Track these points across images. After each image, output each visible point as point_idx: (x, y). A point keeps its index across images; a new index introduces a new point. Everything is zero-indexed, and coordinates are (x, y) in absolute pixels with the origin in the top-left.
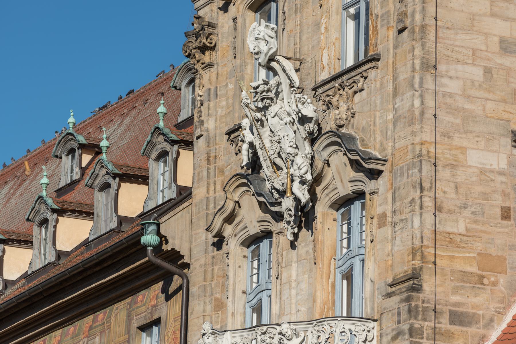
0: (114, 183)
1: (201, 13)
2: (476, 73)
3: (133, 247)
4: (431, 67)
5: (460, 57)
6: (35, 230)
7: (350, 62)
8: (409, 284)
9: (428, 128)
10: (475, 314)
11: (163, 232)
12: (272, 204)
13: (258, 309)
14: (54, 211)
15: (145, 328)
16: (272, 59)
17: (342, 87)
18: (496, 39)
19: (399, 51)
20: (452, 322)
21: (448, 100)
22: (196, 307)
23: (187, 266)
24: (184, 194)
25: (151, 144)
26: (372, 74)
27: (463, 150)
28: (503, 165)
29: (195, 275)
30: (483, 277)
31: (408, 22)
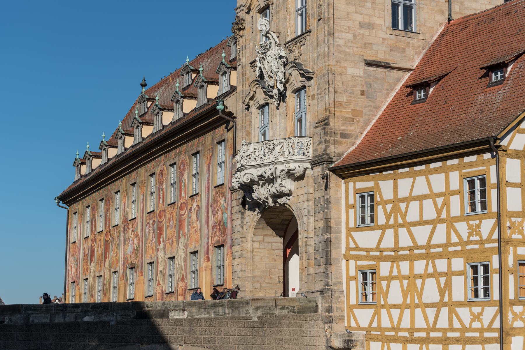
0: (205, 85)
1: (238, 15)
2: (350, 36)
3: (213, 111)
4: (332, 34)
5: (343, 30)
6: (175, 105)
7: (299, 33)
8: (324, 122)
9: (331, 59)
10: (351, 134)
11: (225, 104)
12: (269, 92)
13: (264, 134)
14: (182, 97)
15: (219, 143)
16: (267, 33)
17: (296, 43)
18: (358, 22)
19: (319, 28)
20: (342, 137)
21: (339, 48)
22: (239, 134)
23: (235, 118)
24: (233, 89)
25: (220, 69)
26: (308, 38)
28: (361, 73)
29: (239, 121)
31: (322, 16)
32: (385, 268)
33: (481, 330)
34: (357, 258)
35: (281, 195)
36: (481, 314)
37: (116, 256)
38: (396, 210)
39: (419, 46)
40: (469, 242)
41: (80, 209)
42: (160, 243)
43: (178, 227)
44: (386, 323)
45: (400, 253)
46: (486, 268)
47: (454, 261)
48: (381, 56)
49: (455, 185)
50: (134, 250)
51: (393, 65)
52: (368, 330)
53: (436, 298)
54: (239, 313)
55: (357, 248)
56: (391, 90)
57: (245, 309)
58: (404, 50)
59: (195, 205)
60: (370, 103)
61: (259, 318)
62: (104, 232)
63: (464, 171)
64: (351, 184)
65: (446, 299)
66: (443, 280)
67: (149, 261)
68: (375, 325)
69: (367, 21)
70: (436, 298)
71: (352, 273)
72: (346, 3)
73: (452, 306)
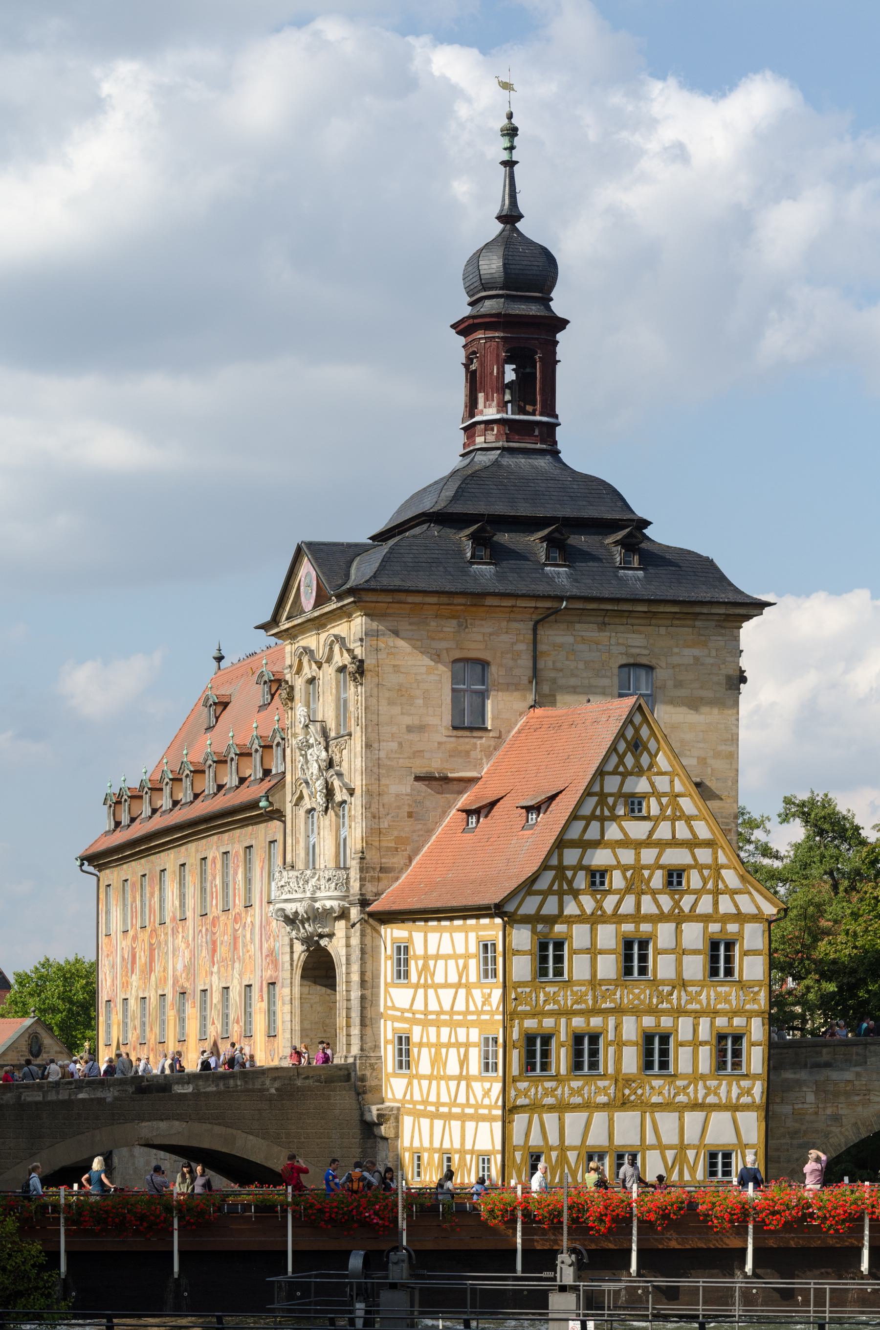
2: (394, 745)
23: (285, 816)
27: (387, 786)
28: (409, 790)
30: (397, 848)
32: (416, 1034)
33: (490, 1107)
34: (394, 1019)
35: (321, 936)
36: (490, 1090)
37: (164, 971)
38: (425, 966)
39: (489, 746)
40: (483, 1012)
41: (115, 881)
42: (214, 964)
43: (232, 944)
44: (417, 1097)
45: (430, 1017)
46: (495, 1040)
47: (471, 1030)
48: (435, 764)
49: (473, 949)
50: (185, 966)
51: (450, 775)
52: (403, 1101)
53: (457, 1072)
54: (253, 1084)
55: (393, 1008)
56: (450, 807)
57: (260, 1080)
58: (467, 753)
59: (249, 920)
60: (420, 826)
61: (277, 1090)
62: (149, 929)
63: (480, 933)
64: (389, 930)
65: (464, 1073)
66: (462, 1050)
67: (203, 988)
68: (408, 1097)
69: (417, 722)
70: (457, 1072)
71: (390, 1036)
72: (389, 704)
73: (468, 1079)
